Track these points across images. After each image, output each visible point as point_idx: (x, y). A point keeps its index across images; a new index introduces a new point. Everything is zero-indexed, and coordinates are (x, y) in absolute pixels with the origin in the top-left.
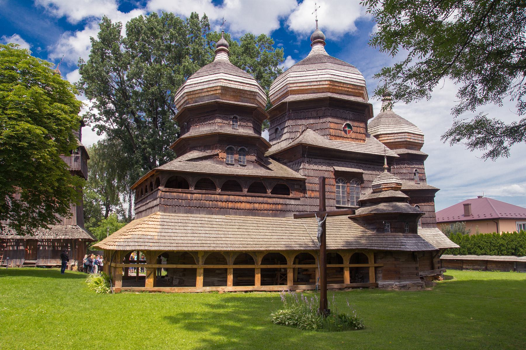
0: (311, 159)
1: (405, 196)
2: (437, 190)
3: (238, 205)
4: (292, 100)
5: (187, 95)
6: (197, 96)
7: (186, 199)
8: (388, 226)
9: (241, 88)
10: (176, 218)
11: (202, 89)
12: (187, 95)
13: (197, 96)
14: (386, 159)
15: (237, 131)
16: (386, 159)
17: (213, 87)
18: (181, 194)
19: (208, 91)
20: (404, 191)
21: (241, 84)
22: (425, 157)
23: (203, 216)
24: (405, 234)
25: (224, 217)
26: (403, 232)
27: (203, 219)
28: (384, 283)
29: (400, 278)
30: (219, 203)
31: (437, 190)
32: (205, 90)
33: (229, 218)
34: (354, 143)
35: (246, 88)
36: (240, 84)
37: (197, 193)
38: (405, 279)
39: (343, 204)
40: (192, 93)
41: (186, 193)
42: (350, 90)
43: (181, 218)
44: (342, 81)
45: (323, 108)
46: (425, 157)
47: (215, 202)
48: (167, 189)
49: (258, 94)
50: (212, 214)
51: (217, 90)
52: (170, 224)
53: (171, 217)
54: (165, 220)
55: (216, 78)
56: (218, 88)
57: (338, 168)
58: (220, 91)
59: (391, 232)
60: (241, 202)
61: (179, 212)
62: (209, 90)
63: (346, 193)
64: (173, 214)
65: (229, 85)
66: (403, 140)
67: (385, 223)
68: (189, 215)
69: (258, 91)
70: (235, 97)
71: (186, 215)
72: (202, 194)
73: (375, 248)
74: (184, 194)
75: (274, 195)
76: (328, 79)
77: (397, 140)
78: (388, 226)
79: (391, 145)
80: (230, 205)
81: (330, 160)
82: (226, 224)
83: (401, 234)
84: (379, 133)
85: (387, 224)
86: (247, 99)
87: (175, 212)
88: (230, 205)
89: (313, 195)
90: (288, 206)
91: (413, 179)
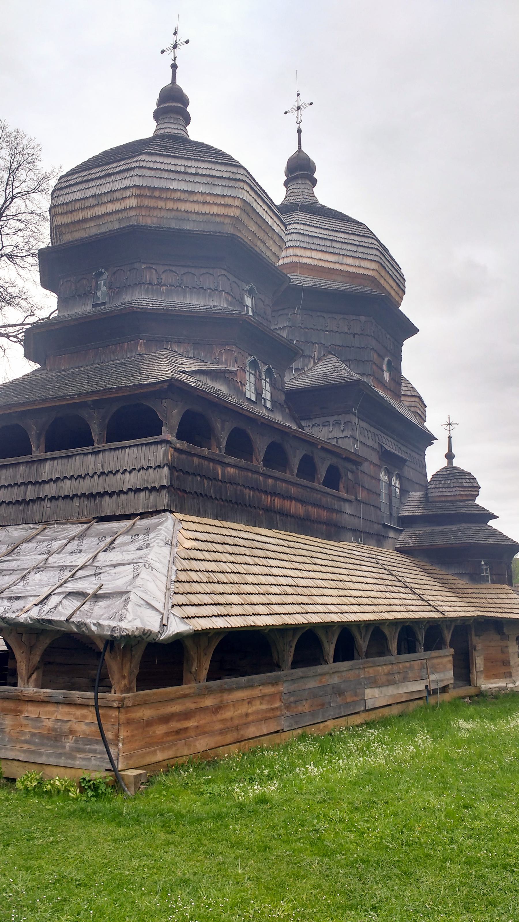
5: (137, 196)
6: (170, 205)
12: (137, 196)
13: (170, 205)
17: (223, 196)
18: (206, 463)
28: (491, 686)
32: (201, 198)
40: (157, 194)
45: (363, 318)
51: (230, 206)
56: (237, 203)
59: (493, 582)
62: (209, 199)
76: (377, 259)
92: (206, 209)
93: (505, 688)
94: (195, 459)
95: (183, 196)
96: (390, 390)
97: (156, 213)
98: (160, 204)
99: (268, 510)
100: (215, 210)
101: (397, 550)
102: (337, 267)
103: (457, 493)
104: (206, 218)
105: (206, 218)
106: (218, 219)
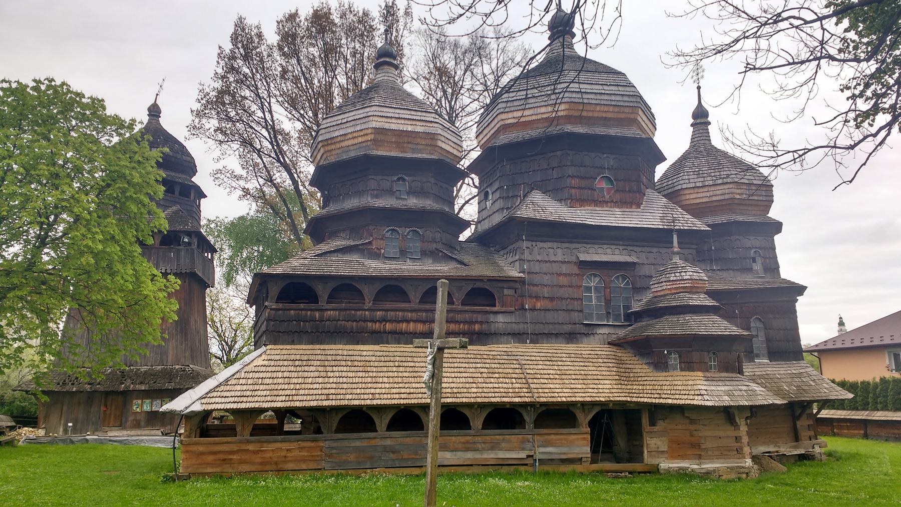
0: (534, 244)
1: (710, 302)
2: (800, 290)
3: (404, 326)
4: (506, 141)
6: (338, 146)
7: (313, 320)
8: (675, 359)
9: (410, 128)
10: (293, 352)
11: (345, 135)
13: (338, 146)
14: (675, 237)
15: (404, 203)
16: (675, 237)
19: (354, 138)
20: (711, 294)
21: (409, 122)
22: (777, 227)
23: (341, 346)
24: (708, 375)
25: (377, 347)
26: (705, 368)
27: (340, 352)
28: (671, 465)
29: (700, 457)
30: (369, 324)
31: (800, 290)
32: (350, 136)
33: (385, 349)
34: (617, 211)
35: (419, 129)
36: (406, 122)
37: (331, 310)
38: (711, 458)
39: (598, 319)
41: (311, 310)
42: (609, 115)
43: (301, 352)
44: (594, 102)
45: (559, 153)
46: (777, 227)
47: (362, 323)
48: (280, 306)
49: (439, 137)
50: (358, 344)
52: (281, 363)
53: (284, 352)
54: (273, 357)
55: (365, 115)
56: (369, 131)
57: (583, 257)
58: (372, 136)
59: (682, 370)
60: (408, 321)
61: (300, 343)
62: (355, 135)
63: (603, 300)
64: (288, 347)
65: (387, 126)
66: (727, 197)
67: (669, 353)
68: (318, 347)
69: (440, 131)
70: (399, 146)
71: (310, 347)
72: (340, 310)
73: (646, 400)
74: (309, 313)
75: (467, 308)
77: (714, 198)
78: (674, 359)
79: (696, 211)
80: (389, 326)
81: (571, 242)
82: (378, 359)
83: (700, 374)
84: (679, 187)
85: (673, 356)
86: (422, 147)
87: (293, 343)
88: (389, 326)
89: (538, 306)
90: (493, 325)
91: (750, 270)
92: (356, 141)
93: (687, 468)
94: (292, 312)
95: (342, 138)
96: (612, 201)
97: (334, 152)
98: (333, 147)
99: (373, 332)
100: (360, 140)
101: (609, 343)
102: (534, 118)
103: (665, 287)
104: (358, 146)
105: (358, 146)
106: (364, 144)
